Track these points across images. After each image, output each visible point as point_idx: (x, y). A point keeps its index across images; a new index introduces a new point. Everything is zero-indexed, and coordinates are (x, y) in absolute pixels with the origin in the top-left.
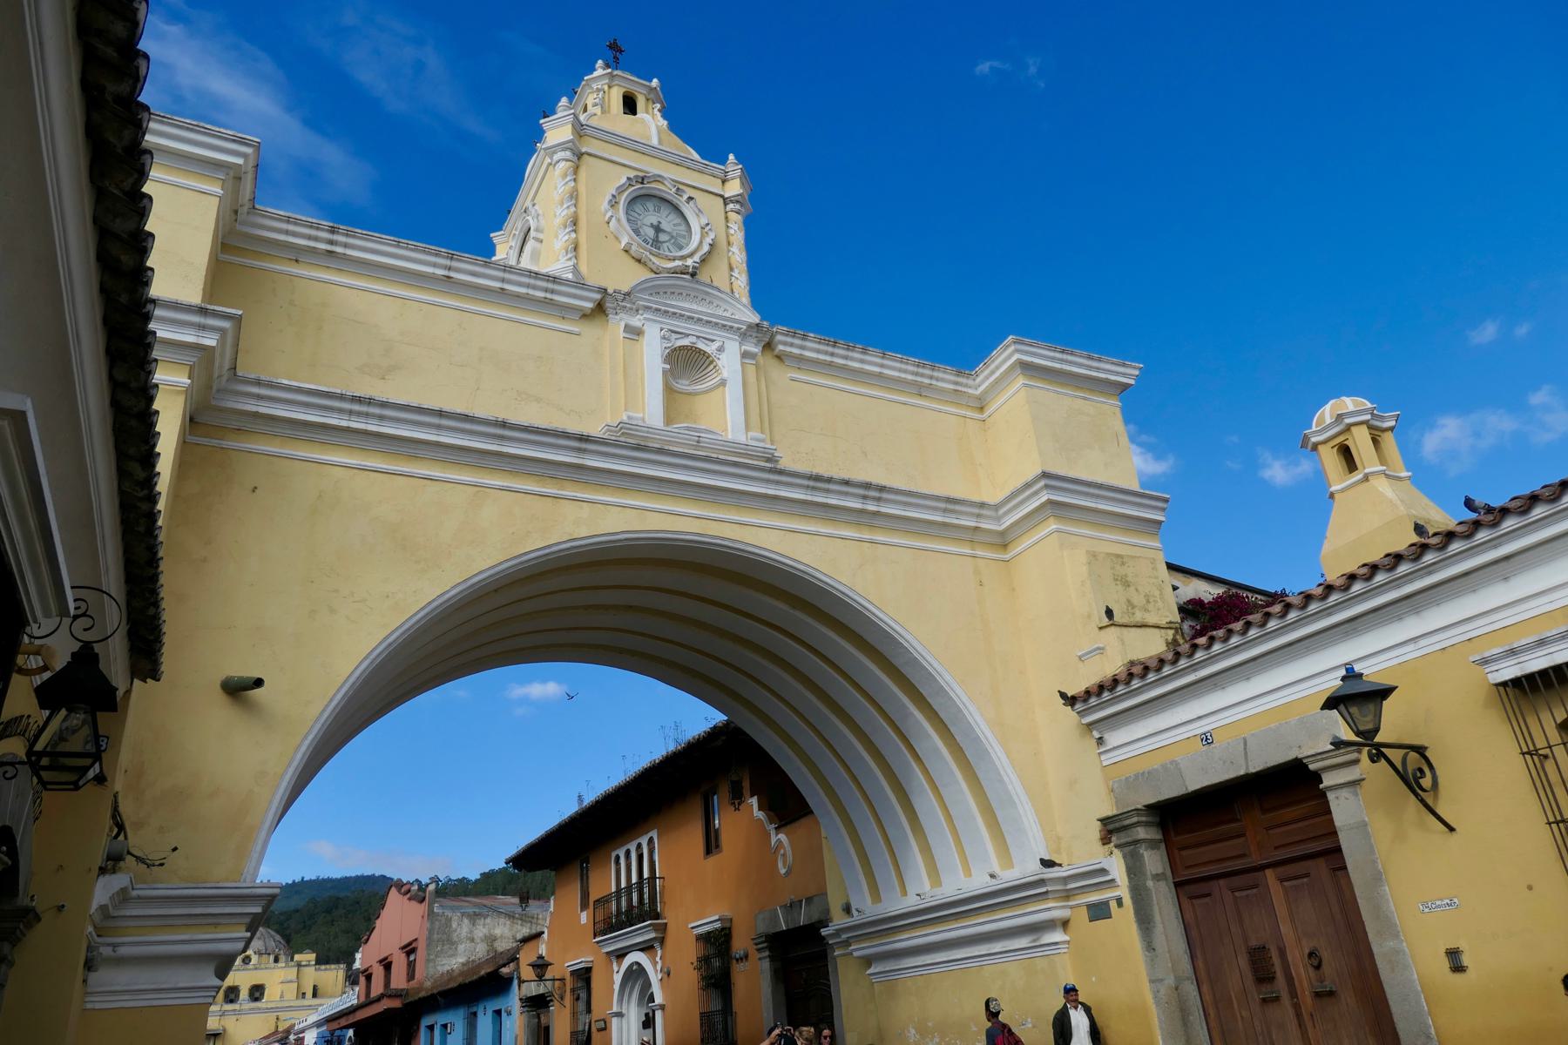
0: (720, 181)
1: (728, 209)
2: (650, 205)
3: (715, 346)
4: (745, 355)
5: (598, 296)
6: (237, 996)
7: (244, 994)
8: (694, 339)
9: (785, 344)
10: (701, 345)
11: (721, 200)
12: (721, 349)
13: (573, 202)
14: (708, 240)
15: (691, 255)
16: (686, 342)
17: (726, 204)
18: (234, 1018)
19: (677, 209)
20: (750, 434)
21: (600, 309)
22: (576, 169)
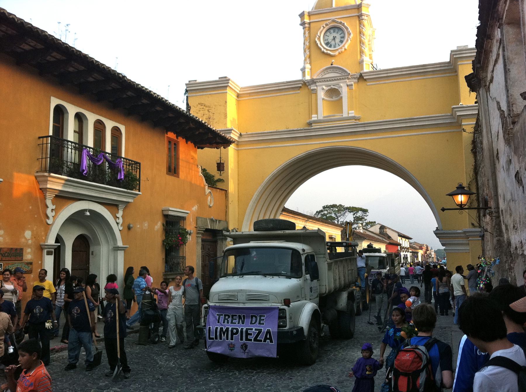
0: (356, 10)
1: (360, 19)
2: (332, 31)
4: (347, 86)
11: (357, 17)
13: (308, 41)
16: (329, 88)
17: (359, 18)
19: (339, 29)
20: (350, 112)
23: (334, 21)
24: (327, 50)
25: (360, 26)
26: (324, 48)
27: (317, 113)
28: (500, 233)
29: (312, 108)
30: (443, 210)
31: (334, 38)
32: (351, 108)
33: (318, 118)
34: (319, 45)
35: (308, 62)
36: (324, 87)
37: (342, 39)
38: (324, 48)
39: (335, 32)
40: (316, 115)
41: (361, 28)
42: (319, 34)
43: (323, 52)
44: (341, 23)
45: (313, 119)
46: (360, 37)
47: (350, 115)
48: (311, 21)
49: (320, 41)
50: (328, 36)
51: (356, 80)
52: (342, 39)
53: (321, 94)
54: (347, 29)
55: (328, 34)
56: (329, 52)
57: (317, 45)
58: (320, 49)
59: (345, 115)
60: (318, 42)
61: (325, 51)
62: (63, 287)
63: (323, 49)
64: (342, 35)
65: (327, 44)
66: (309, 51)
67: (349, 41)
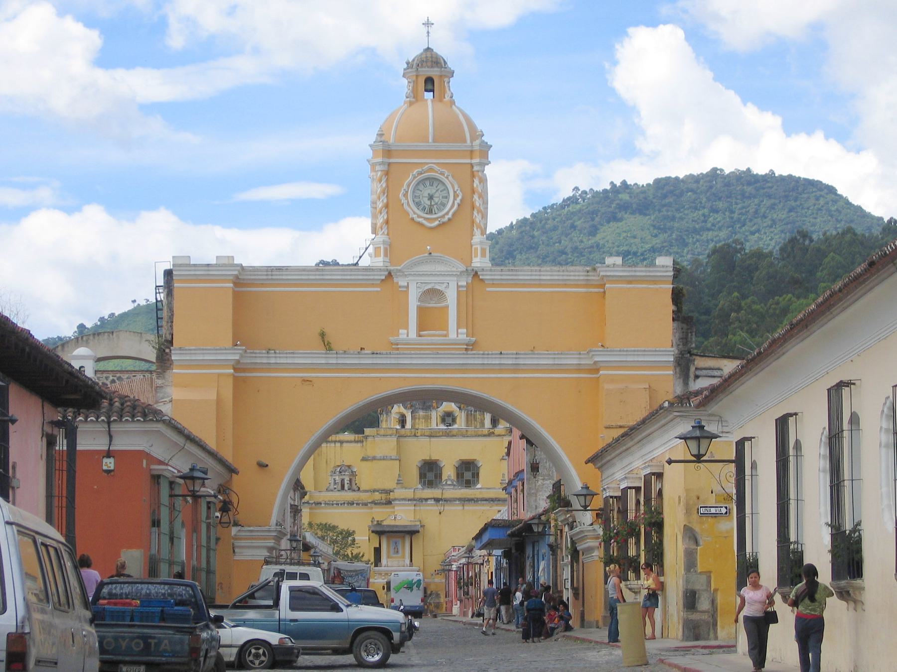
3: (445, 285)
4: (458, 286)
5: (386, 273)
6: (439, 476)
7: (449, 472)
8: (433, 285)
9: (482, 275)
10: (437, 287)
11: (469, 166)
12: (447, 287)
13: (386, 195)
14: (458, 200)
15: (447, 213)
16: (429, 286)
18: (437, 508)
20: (459, 331)
21: (390, 275)
22: (387, 173)
23: (431, 170)
24: (419, 216)
25: (473, 181)
26: (415, 213)
31: (431, 198)
33: (408, 336)
34: (405, 206)
35: (386, 233)
38: (415, 213)
39: (432, 185)
40: (406, 331)
41: (475, 185)
42: (405, 187)
43: (413, 219)
45: (401, 337)
47: (460, 337)
48: (392, 160)
49: (407, 199)
50: (421, 191)
51: (470, 279)
52: (445, 201)
55: (421, 187)
60: (404, 201)
63: (412, 215)
64: (444, 193)
65: (418, 204)
66: (387, 212)
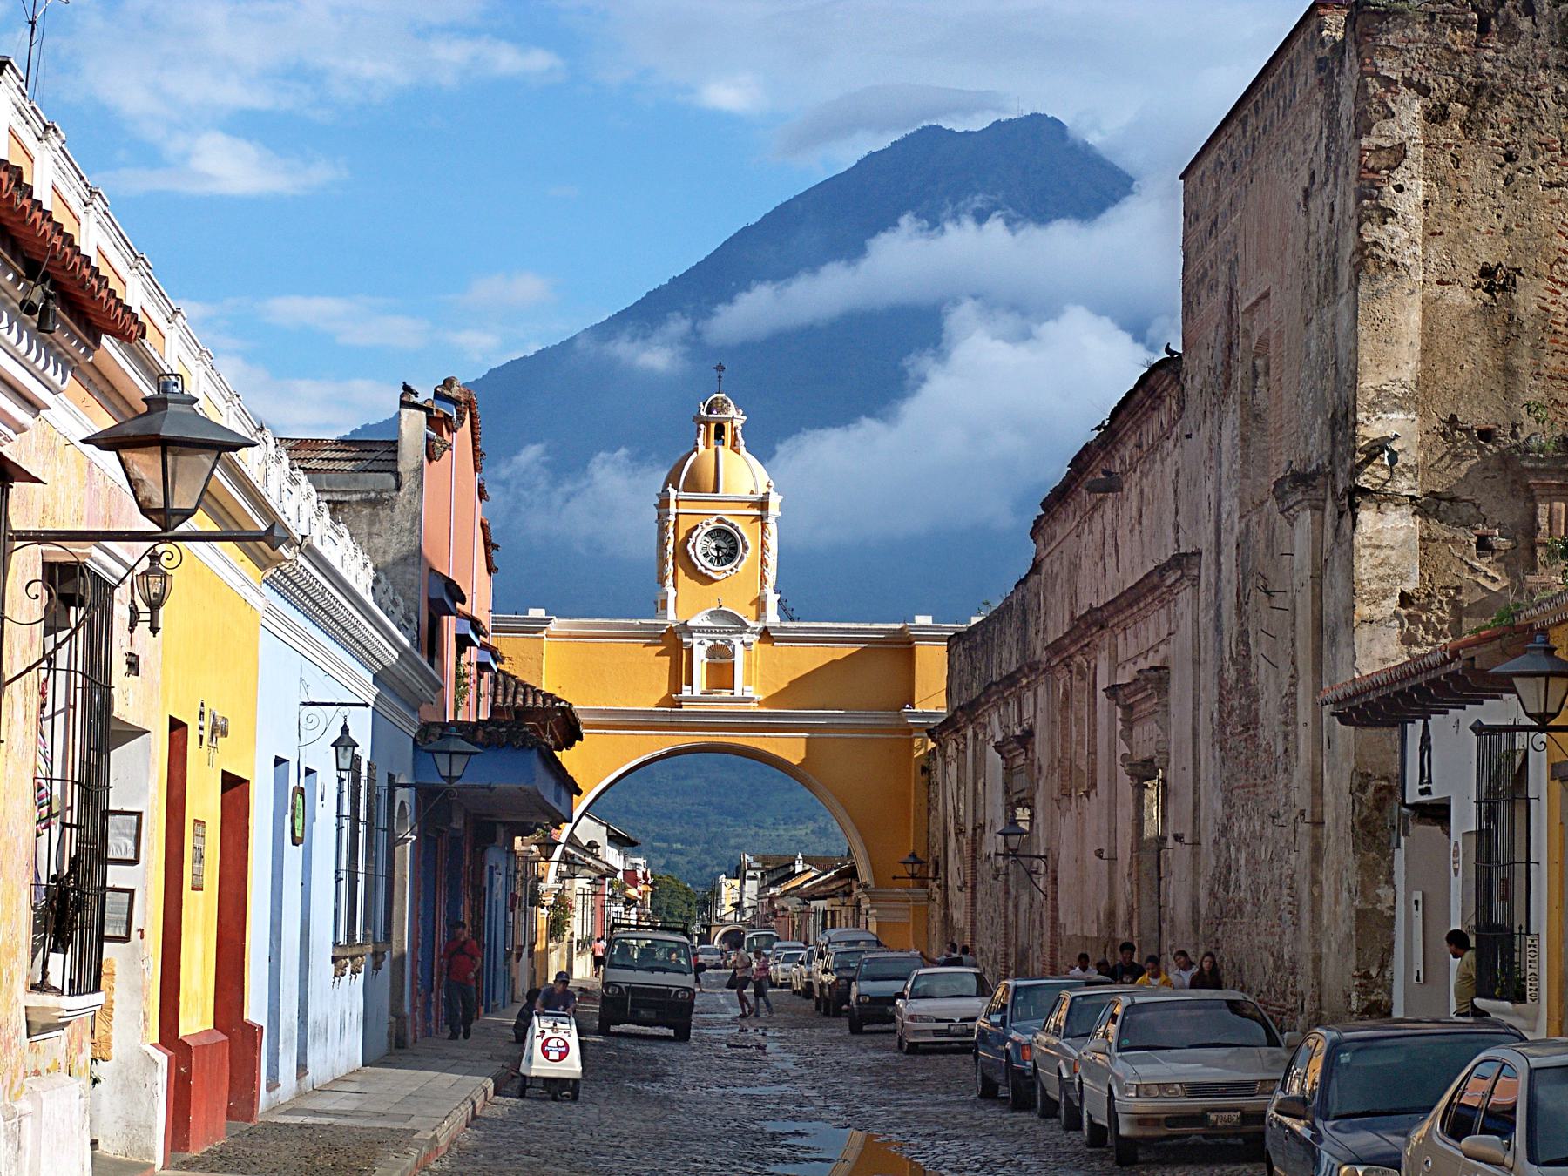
20: (746, 688)
27: (690, 683)
28: (946, 907)
29: (680, 673)
30: (894, 878)
32: (748, 682)
34: (693, 558)
36: (705, 640)
37: (732, 552)
44: (732, 525)
46: (763, 554)
48: (680, 511)
53: (700, 654)
54: (742, 538)
56: (709, 573)
57: (689, 557)
58: (696, 566)
59: (738, 693)
60: (692, 552)
61: (704, 571)
62: (538, 947)
63: (700, 567)
65: (706, 555)
67: (745, 560)
